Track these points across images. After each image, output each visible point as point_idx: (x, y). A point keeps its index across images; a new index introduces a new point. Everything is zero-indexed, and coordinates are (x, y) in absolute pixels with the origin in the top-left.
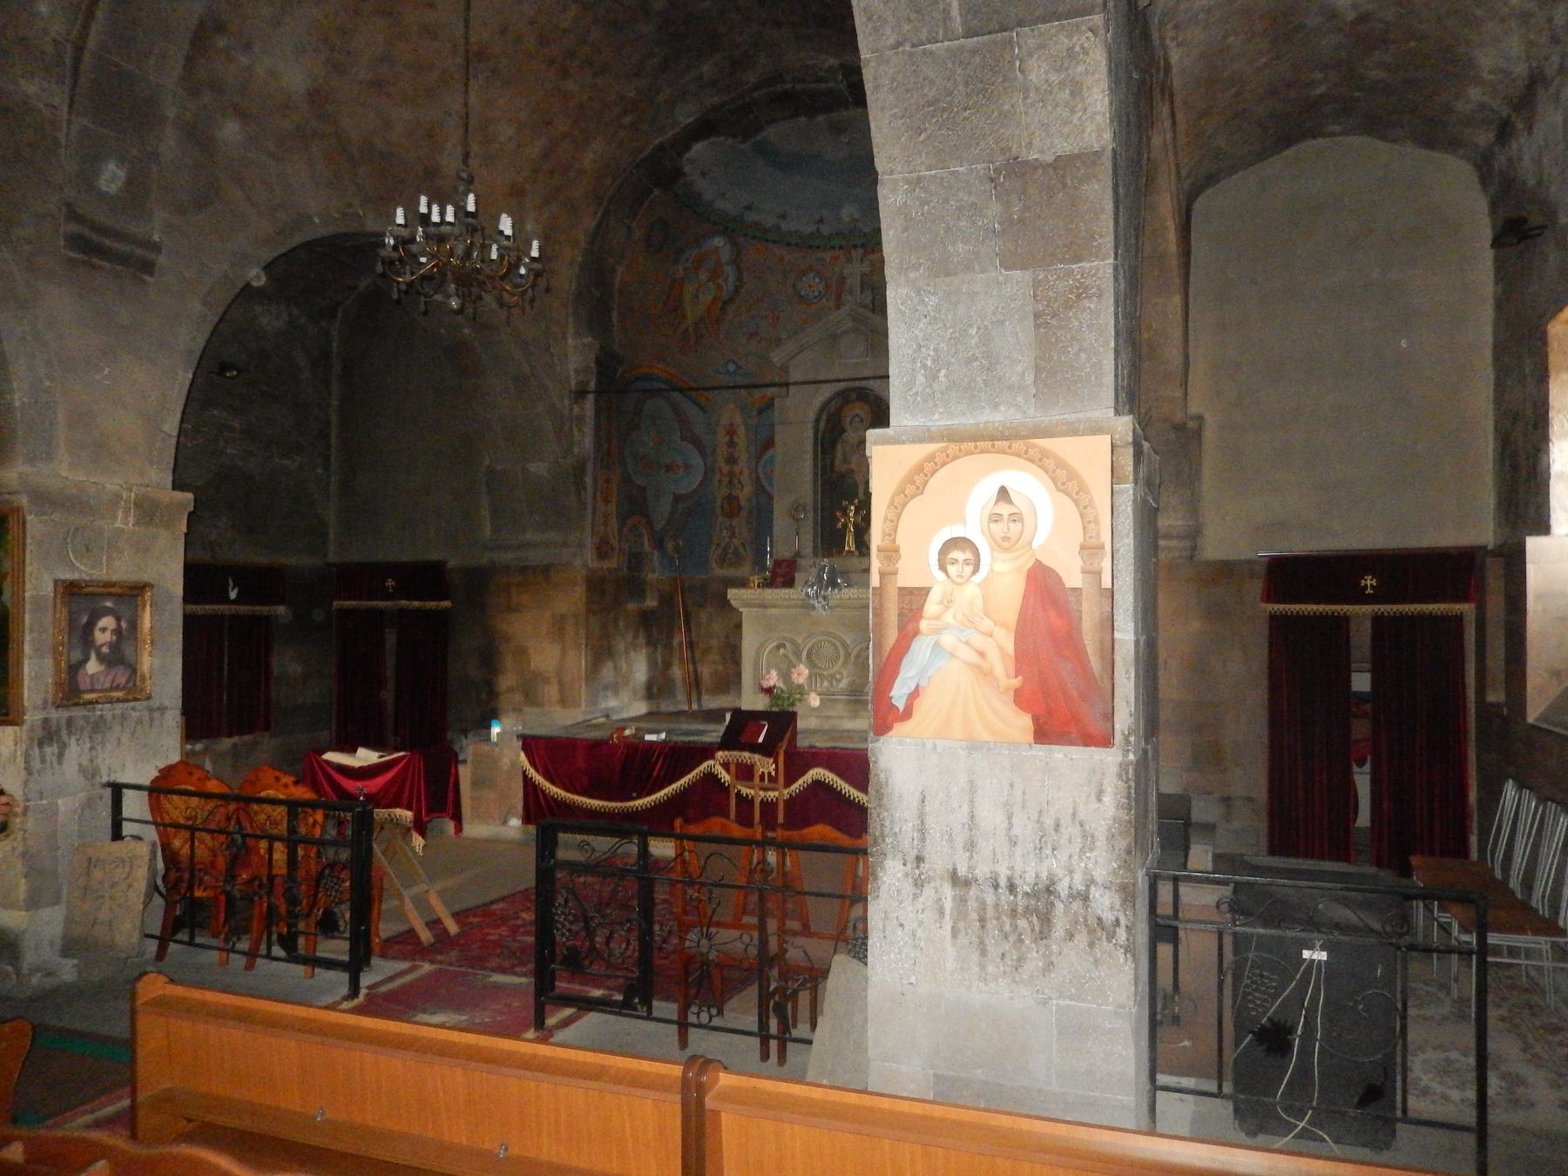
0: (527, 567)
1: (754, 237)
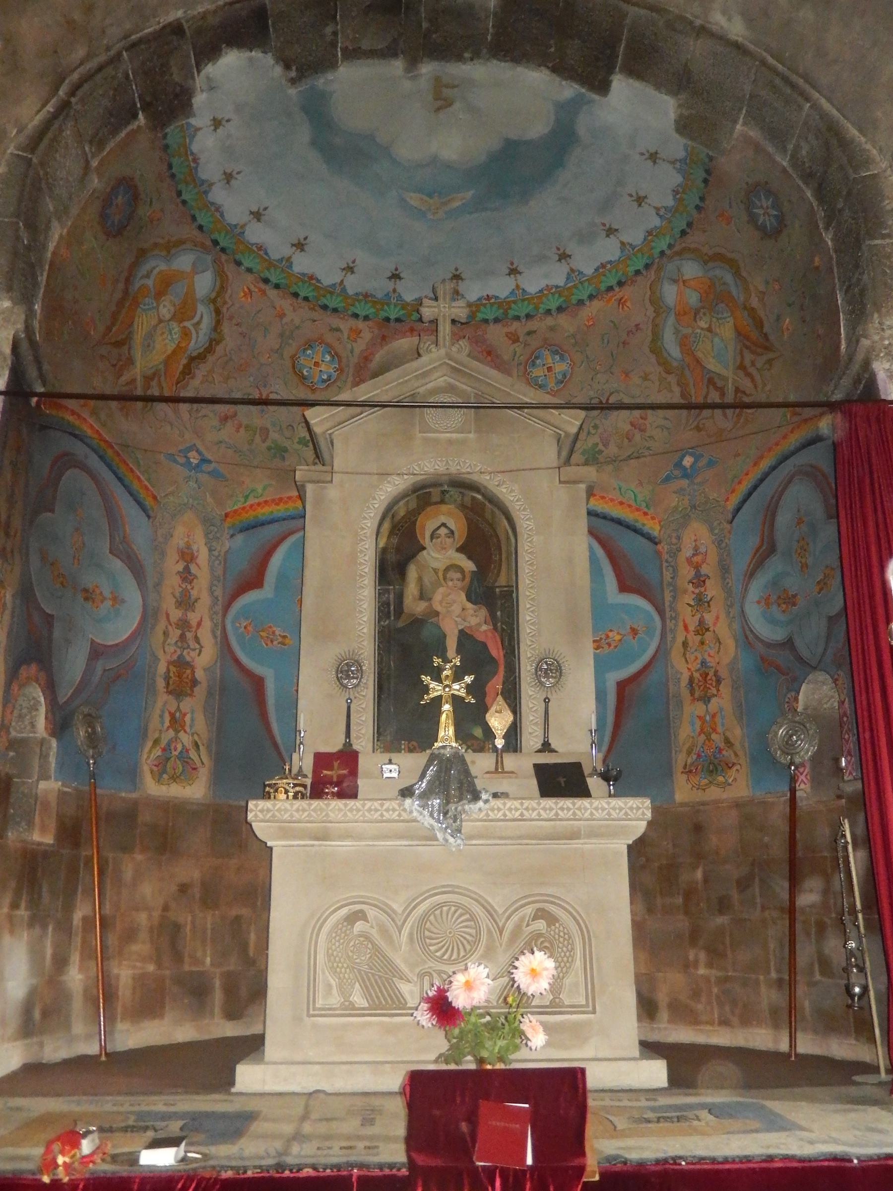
1: (249, 270)
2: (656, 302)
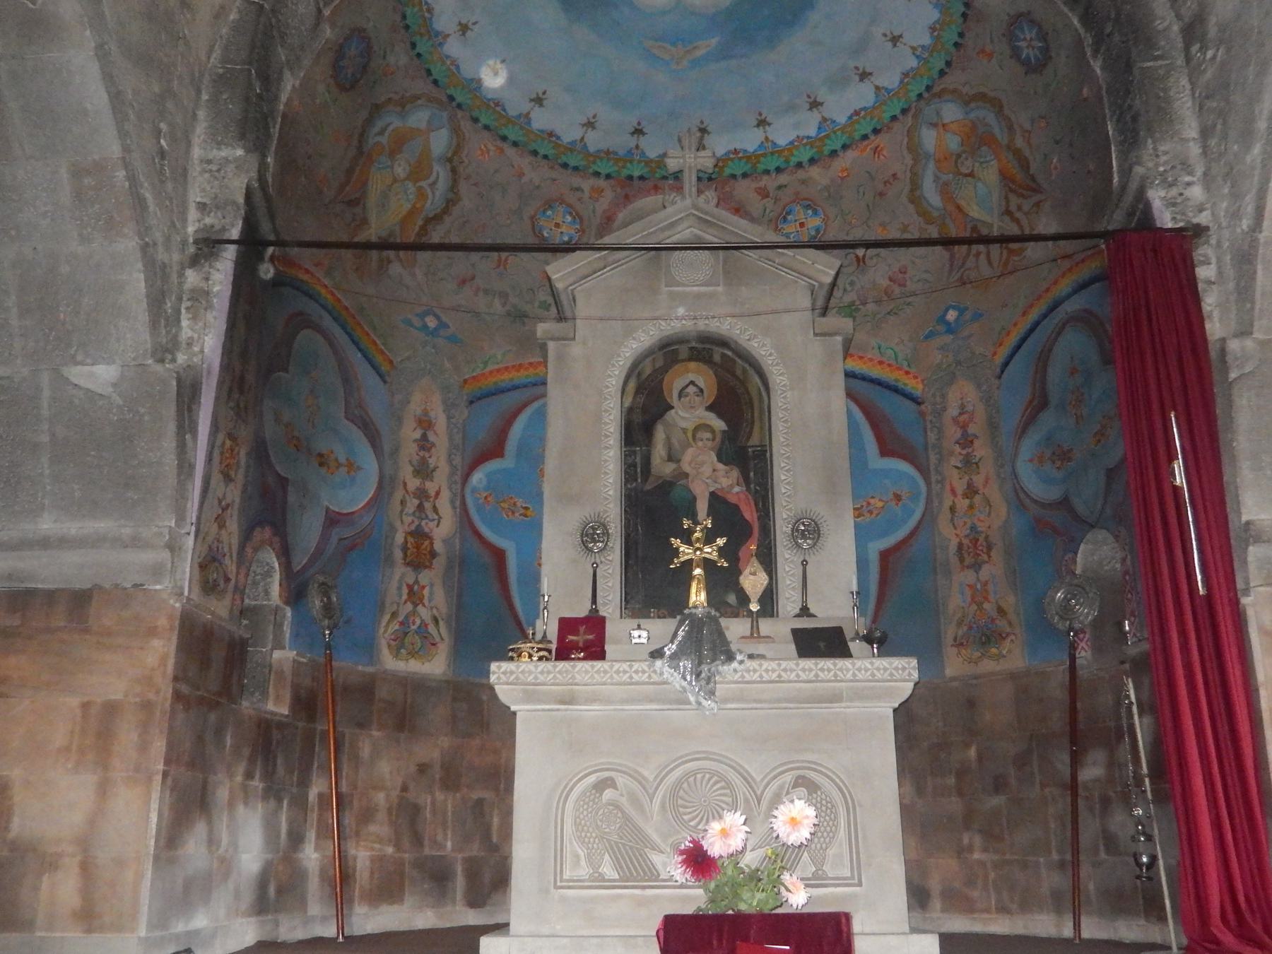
0: (31, 593)
1: (487, 127)
2: (914, 148)
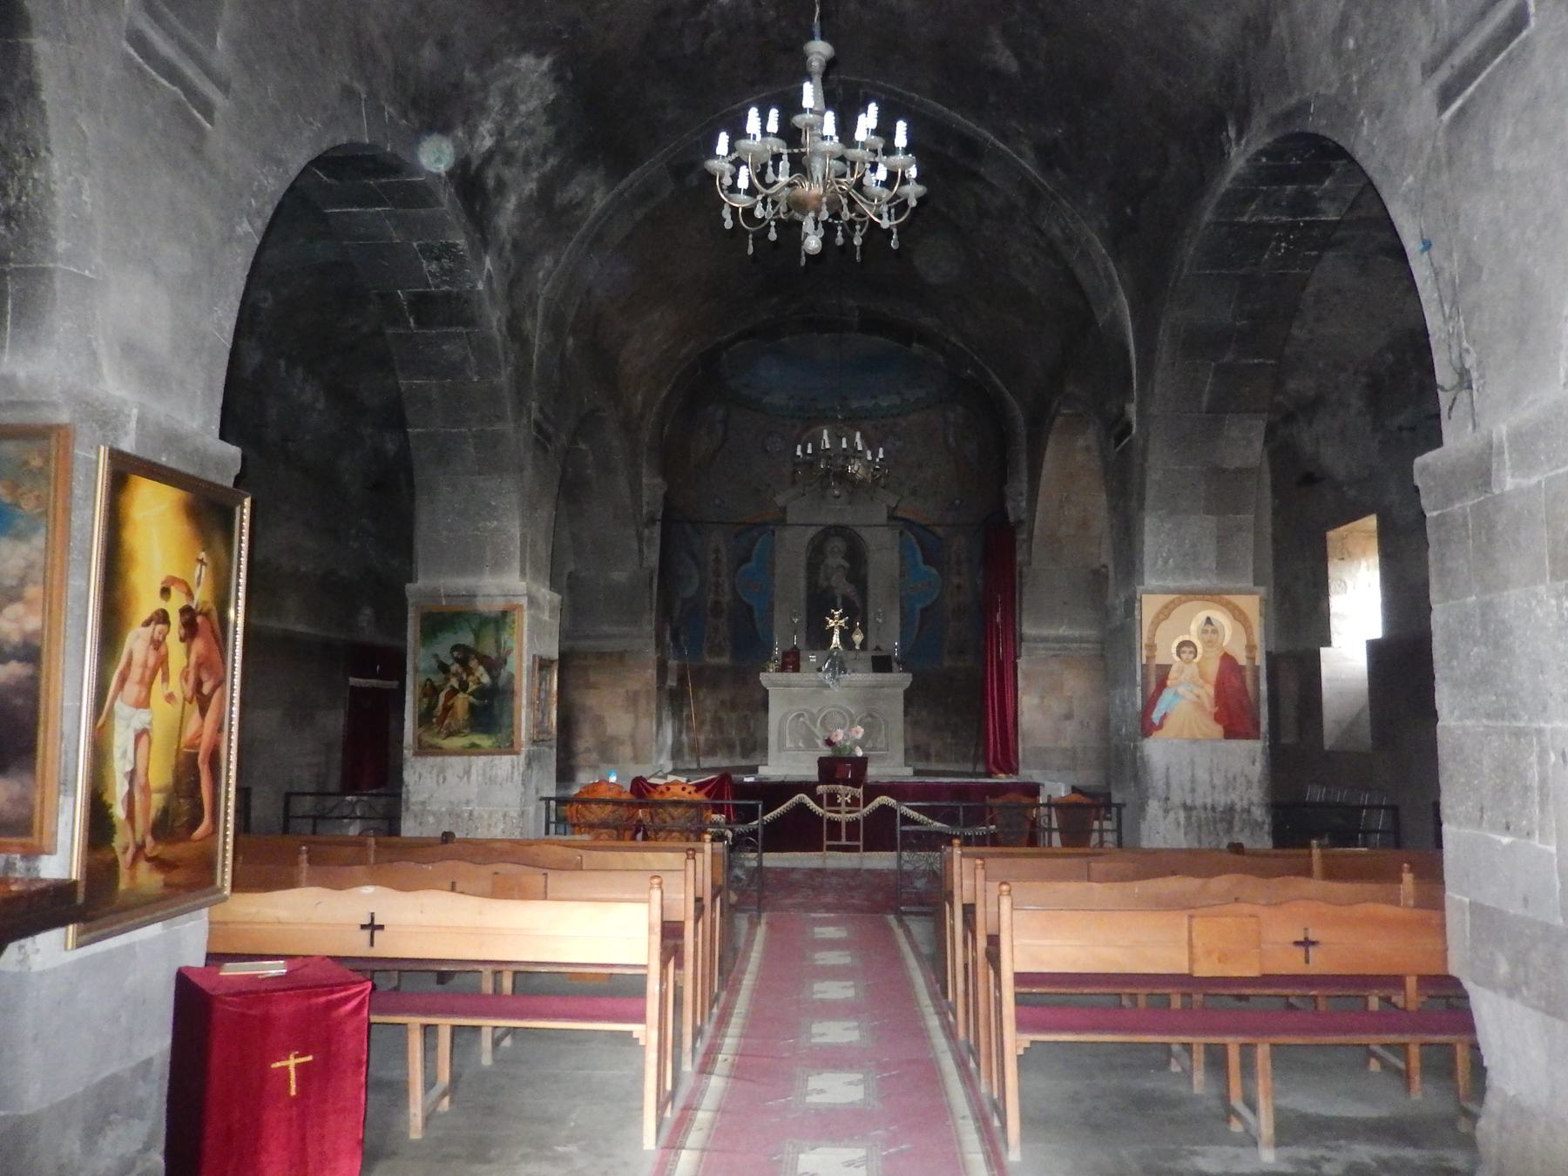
0: (603, 654)
